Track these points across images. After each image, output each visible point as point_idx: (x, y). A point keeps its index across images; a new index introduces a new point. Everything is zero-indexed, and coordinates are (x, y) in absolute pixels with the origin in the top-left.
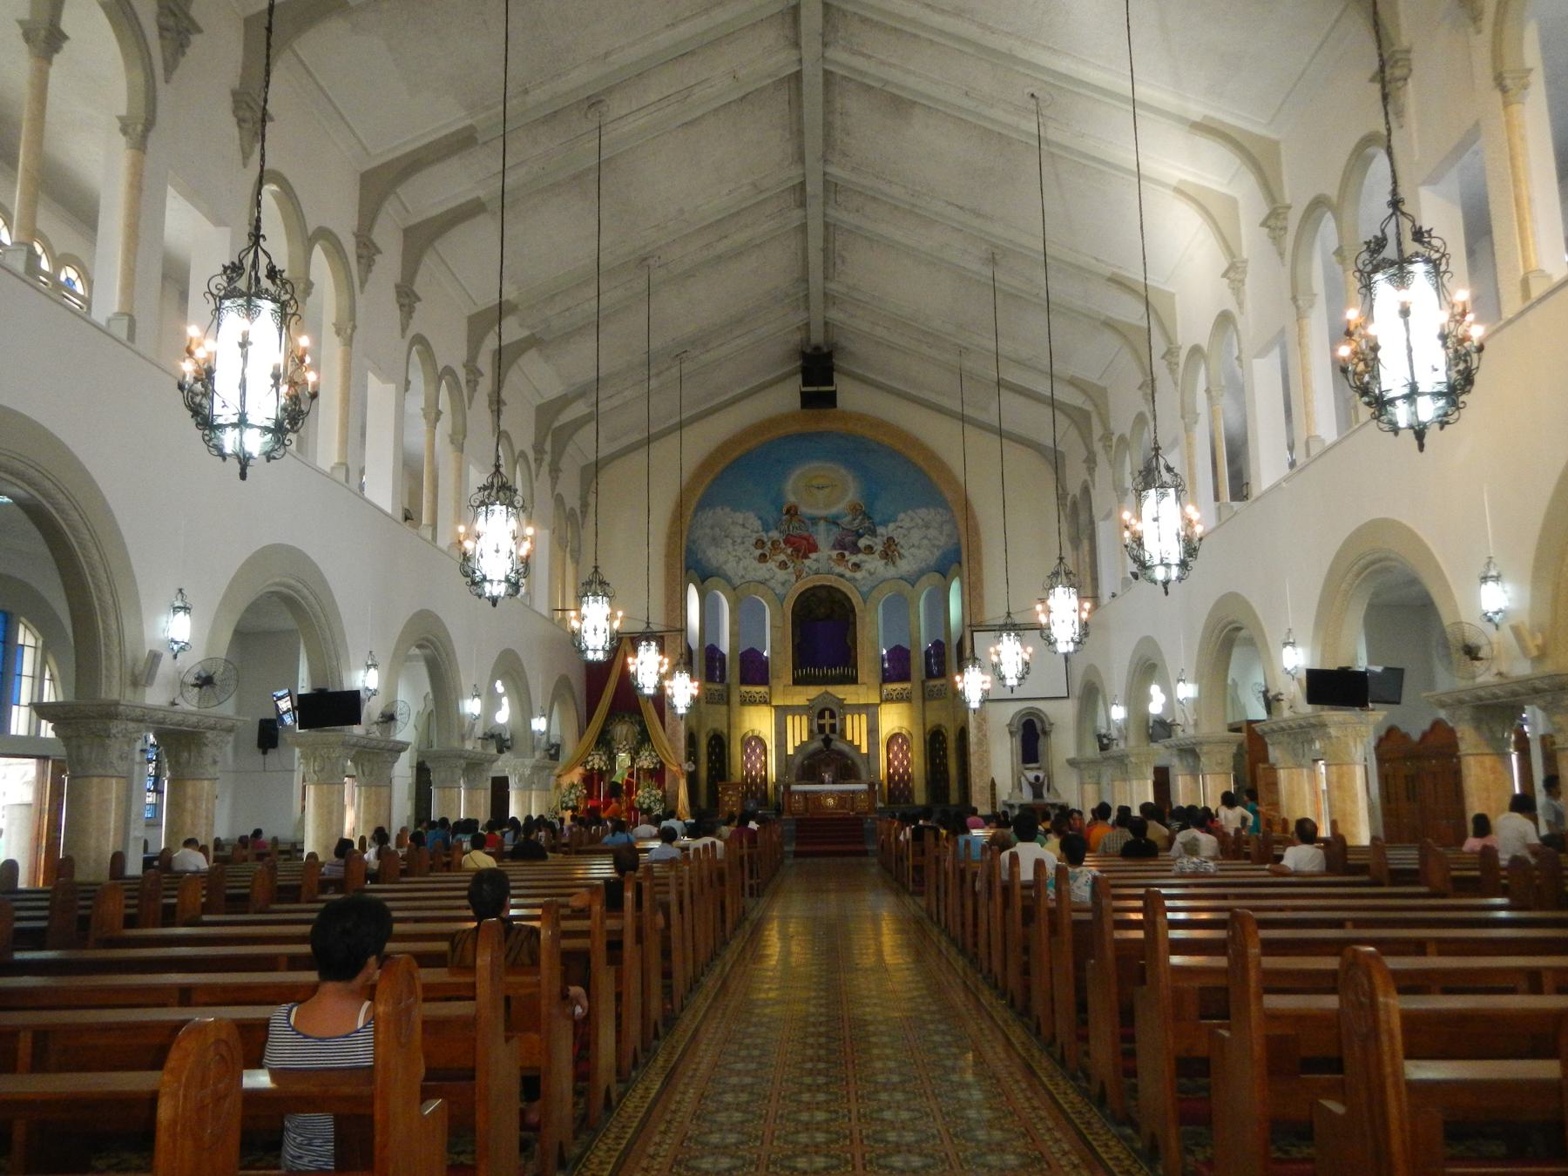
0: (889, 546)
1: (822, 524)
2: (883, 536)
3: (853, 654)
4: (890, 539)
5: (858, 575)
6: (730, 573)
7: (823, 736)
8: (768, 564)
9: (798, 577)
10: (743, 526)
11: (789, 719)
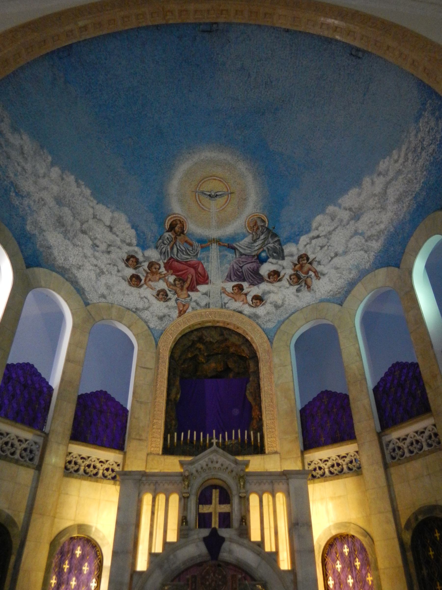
0: (302, 267)
1: (214, 246)
2: (292, 255)
3: (255, 414)
4: (303, 257)
5: (261, 311)
6: (83, 284)
7: (205, 532)
8: (142, 290)
9: (181, 313)
10: (111, 228)
11: (147, 499)
